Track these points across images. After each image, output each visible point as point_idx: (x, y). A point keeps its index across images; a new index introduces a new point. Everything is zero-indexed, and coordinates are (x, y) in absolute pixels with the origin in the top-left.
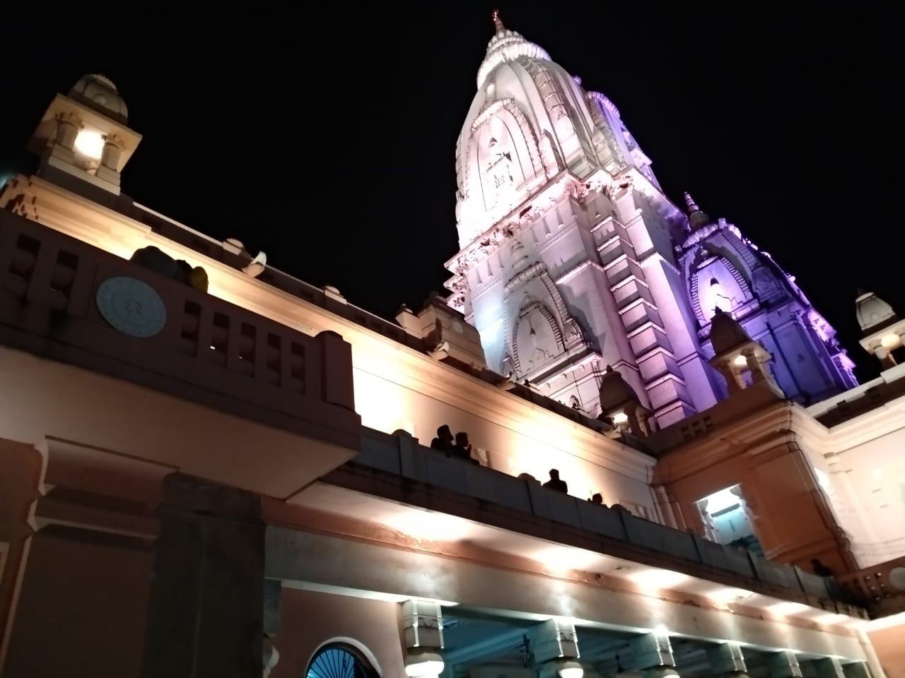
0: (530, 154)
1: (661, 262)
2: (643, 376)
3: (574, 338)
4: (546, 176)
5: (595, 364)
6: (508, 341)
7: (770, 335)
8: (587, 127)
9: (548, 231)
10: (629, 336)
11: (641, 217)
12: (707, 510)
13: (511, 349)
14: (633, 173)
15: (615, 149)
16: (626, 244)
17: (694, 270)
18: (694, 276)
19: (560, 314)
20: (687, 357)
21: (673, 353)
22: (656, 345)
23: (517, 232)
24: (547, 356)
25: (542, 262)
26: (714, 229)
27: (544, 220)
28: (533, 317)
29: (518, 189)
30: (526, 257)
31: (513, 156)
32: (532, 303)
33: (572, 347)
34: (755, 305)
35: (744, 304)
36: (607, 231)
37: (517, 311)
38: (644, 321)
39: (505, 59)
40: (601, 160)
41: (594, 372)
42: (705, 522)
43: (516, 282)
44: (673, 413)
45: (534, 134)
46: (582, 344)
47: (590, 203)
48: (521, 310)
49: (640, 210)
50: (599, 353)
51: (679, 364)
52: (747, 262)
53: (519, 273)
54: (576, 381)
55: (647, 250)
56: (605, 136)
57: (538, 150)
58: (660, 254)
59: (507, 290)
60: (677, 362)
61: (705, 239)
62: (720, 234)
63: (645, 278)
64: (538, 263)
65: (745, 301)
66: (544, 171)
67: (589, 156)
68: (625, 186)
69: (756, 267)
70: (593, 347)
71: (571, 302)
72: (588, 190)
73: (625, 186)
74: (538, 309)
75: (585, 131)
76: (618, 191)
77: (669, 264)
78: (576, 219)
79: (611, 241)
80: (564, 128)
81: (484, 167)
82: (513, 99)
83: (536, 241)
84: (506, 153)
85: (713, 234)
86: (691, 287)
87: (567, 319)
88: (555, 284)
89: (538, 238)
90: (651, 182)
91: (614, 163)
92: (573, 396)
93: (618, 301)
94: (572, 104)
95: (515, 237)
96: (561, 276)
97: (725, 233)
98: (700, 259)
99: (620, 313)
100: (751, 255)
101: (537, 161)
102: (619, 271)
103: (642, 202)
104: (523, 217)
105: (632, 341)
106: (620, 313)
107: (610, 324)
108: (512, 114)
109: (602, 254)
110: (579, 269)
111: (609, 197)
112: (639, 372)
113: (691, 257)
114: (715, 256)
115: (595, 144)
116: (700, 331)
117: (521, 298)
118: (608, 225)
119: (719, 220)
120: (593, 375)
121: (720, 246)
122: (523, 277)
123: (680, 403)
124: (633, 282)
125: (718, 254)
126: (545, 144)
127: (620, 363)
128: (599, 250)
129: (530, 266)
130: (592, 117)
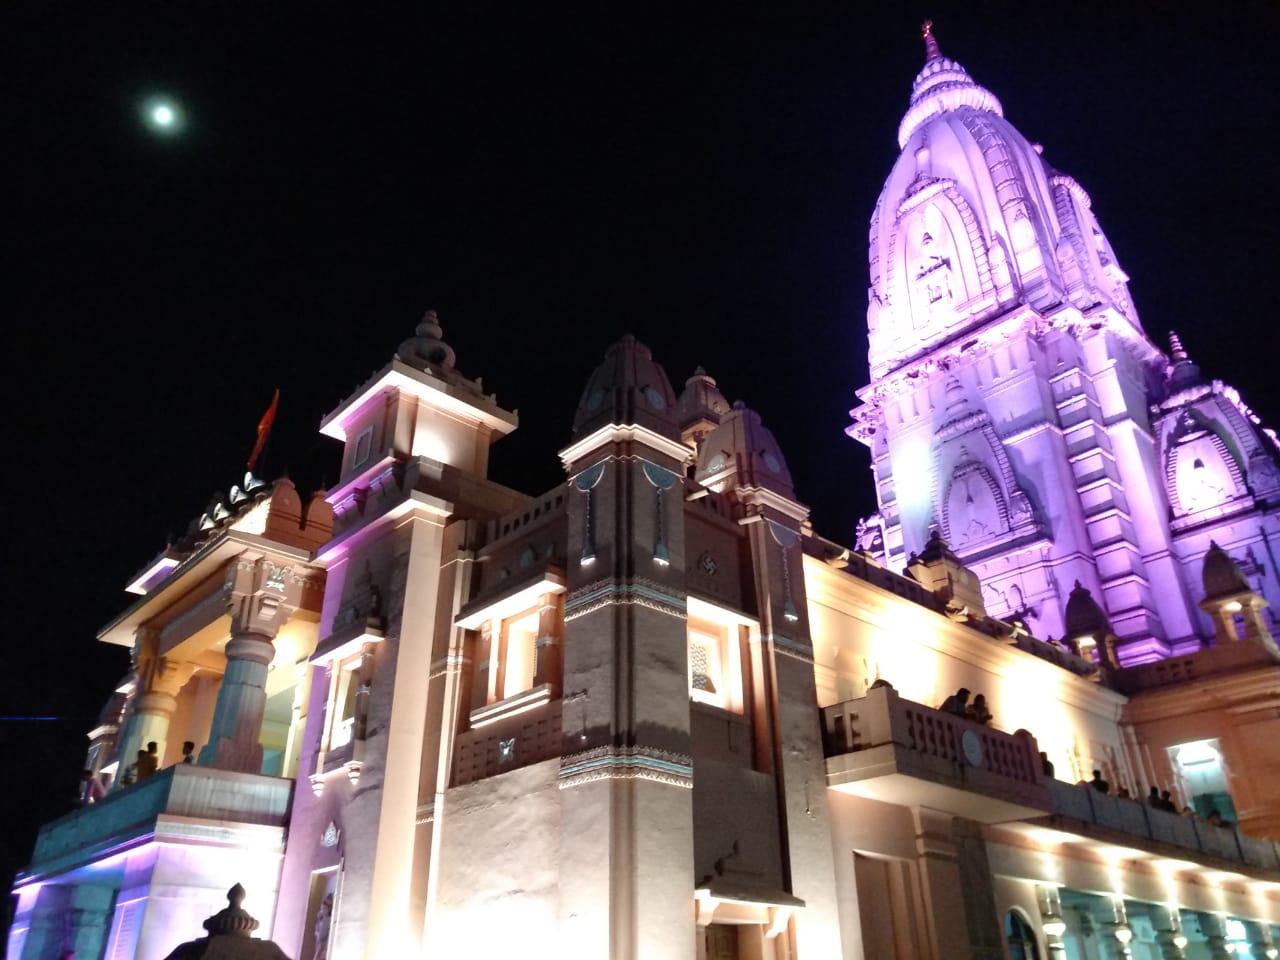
0: (971, 257)
1: (1135, 431)
2: (1101, 572)
3: (1022, 516)
4: (997, 300)
5: (1045, 552)
6: (935, 503)
7: (1262, 543)
8: (1051, 230)
9: (996, 375)
10: (1088, 521)
11: (1113, 370)
12: (1178, 758)
13: (940, 513)
14: (1110, 313)
15: (1086, 267)
16: (1093, 404)
17: (1174, 442)
18: (1173, 450)
19: (1006, 485)
20: (1152, 555)
21: (1137, 547)
22: (1120, 538)
23: (955, 368)
24: (986, 530)
25: (987, 412)
26: (1205, 391)
27: (991, 357)
28: (971, 481)
29: (959, 308)
30: (966, 401)
31: (954, 263)
32: (970, 463)
33: (1019, 527)
34: (1249, 503)
35: (1236, 499)
36: (1071, 386)
37: (950, 469)
38: (1108, 506)
39: (942, 108)
40: (1067, 281)
41: (1043, 561)
42: (1175, 770)
43: (951, 430)
44: (1133, 621)
45: (983, 238)
46: (1031, 527)
47: (1051, 344)
48: (957, 468)
49: (1114, 361)
50: (1051, 539)
51: (1145, 560)
52: (1245, 443)
53: (955, 421)
54: (1020, 568)
55: (1118, 412)
56: (1075, 250)
57: (988, 262)
58: (1134, 420)
59: (937, 438)
60: (1143, 557)
61: (1192, 403)
62: (1213, 401)
63: (1111, 448)
64: (980, 412)
65: (1236, 495)
66: (994, 293)
67: (1055, 280)
68: (1097, 327)
69: (1255, 454)
70: (1044, 531)
71: (1020, 469)
72: (1050, 328)
73: (1097, 327)
74: (978, 472)
75: (1049, 239)
76: (1085, 330)
77: (1142, 433)
78: (1035, 368)
79: (1075, 399)
80: (1022, 233)
81: (914, 271)
82: (955, 182)
83: (980, 383)
84: (944, 258)
85: (1203, 399)
86: (1166, 467)
87: (1014, 491)
88: (1001, 444)
89: (983, 380)
90: (1130, 322)
91: (1083, 290)
92: (1015, 586)
93: (1077, 476)
94: (1034, 198)
95: (951, 372)
96: (1010, 434)
97: (1219, 400)
98: (1181, 430)
99: (1080, 491)
100: (1246, 428)
101: (986, 277)
102: (1082, 438)
103: (1120, 350)
104: (965, 352)
105: (1090, 526)
106: (1080, 491)
107: (1068, 506)
108: (956, 205)
109: (1062, 413)
110: (1033, 431)
111: (1075, 337)
112: (1095, 565)
113: (1170, 423)
114: (1203, 430)
115: (1061, 259)
116: (1173, 522)
117: (954, 453)
118: (1072, 378)
119: (1214, 382)
120: (1042, 564)
121: (1210, 417)
122: (960, 426)
123: (1143, 612)
124: (1099, 456)
125: (1208, 428)
126: (998, 254)
127: (1076, 556)
128: (1059, 407)
129: (971, 415)
130: (1058, 216)
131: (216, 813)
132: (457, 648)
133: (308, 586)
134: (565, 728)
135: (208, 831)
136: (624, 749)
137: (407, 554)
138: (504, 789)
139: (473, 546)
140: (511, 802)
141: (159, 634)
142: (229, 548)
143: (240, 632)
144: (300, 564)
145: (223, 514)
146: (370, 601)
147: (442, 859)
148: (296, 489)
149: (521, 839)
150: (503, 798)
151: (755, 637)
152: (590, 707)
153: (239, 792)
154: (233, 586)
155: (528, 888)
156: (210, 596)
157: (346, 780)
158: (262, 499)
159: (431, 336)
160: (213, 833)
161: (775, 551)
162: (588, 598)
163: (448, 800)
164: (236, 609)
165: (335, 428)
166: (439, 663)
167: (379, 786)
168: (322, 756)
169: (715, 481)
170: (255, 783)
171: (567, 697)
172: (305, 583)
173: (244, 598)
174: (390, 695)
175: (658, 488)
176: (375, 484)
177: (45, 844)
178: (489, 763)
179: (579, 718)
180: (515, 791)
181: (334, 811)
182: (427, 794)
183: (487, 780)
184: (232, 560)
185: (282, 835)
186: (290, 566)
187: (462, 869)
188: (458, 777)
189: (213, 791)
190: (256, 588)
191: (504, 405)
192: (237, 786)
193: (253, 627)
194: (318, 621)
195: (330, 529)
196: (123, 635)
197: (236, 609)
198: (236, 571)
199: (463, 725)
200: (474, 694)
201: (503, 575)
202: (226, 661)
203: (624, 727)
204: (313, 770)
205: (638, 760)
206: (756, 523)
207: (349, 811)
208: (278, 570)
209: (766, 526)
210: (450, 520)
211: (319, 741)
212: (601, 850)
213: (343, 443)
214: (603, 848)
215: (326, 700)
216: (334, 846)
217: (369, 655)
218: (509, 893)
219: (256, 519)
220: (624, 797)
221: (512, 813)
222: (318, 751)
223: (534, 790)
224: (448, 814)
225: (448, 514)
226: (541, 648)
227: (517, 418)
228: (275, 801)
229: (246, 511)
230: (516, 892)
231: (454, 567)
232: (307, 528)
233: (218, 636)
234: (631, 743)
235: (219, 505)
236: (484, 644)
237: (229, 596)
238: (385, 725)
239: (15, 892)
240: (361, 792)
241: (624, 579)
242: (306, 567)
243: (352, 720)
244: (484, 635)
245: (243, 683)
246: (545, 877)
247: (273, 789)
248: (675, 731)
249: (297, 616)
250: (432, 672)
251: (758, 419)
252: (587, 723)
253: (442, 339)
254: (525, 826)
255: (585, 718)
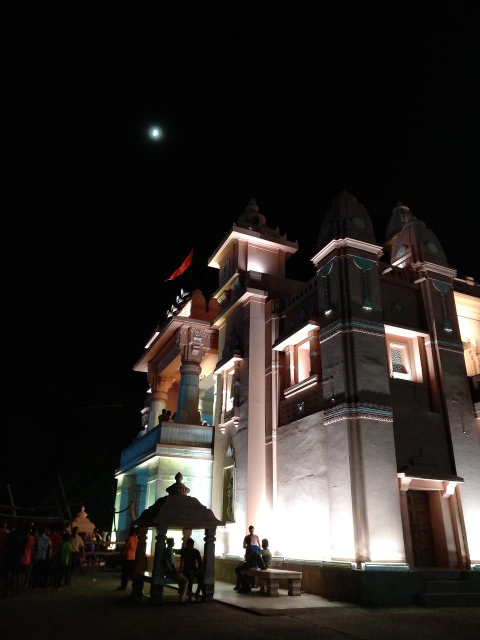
131: (182, 443)
132: (276, 361)
133: (212, 338)
134: (324, 397)
135: (179, 451)
136: (353, 404)
137: (249, 318)
138: (301, 427)
139: (278, 311)
140: (305, 433)
141: (157, 365)
142: (175, 324)
143: (185, 362)
144: (207, 328)
145: (175, 310)
146: (235, 343)
147: (278, 462)
148: (203, 294)
149: (310, 450)
150: (301, 431)
151: (428, 343)
152: (335, 385)
153: (190, 434)
154: (179, 341)
155: (314, 474)
156: (172, 347)
157: (232, 426)
158: (189, 300)
159: (253, 211)
160: (181, 452)
161: (436, 295)
162: (329, 331)
163: (278, 434)
164: (182, 351)
165: (214, 264)
166: (268, 369)
167: (246, 428)
168: (223, 415)
169: (399, 263)
170: (197, 429)
171: (324, 380)
172: (211, 337)
173: (185, 346)
174: (247, 385)
175: (363, 270)
176: (232, 287)
177: (124, 458)
178: (294, 414)
179: (330, 390)
180: (306, 427)
181: (230, 441)
182: (269, 431)
183: (294, 423)
184: (178, 330)
185: (210, 452)
186: (205, 329)
187: (287, 466)
188: (282, 421)
189: (179, 433)
190: (189, 341)
191: (289, 240)
192: (189, 430)
193: (190, 358)
194: (217, 353)
195: (218, 310)
196: (143, 368)
197: (182, 351)
198: (180, 334)
199: (282, 397)
200: (285, 382)
201: (293, 323)
202: (180, 375)
203: (352, 393)
204: (220, 423)
205: (361, 409)
206: (424, 281)
207: (235, 440)
208: (198, 332)
209: (431, 282)
210: (267, 300)
211: (221, 408)
212: (344, 455)
213: (219, 269)
214: (345, 454)
215: (222, 389)
216: (230, 457)
217: (237, 367)
218: (307, 476)
219: (186, 311)
220: (354, 427)
221: (306, 438)
222: (221, 413)
223: (314, 426)
224: (278, 440)
225: (266, 297)
226: (312, 357)
227: (297, 245)
228: (207, 437)
229: (183, 307)
230: (310, 476)
231: (270, 322)
232: (209, 311)
233: (176, 365)
234: (356, 401)
235: (173, 306)
236: (287, 358)
237: (178, 346)
238: (247, 399)
239: (116, 478)
240: (240, 431)
241: (347, 319)
242: (210, 329)
243: (233, 398)
244: (287, 353)
245: (188, 385)
246: (322, 469)
247: (205, 431)
248: (380, 394)
249: (210, 352)
250: (266, 373)
251: (424, 225)
252: (334, 392)
253: (260, 211)
254: (311, 444)
255: (333, 390)
